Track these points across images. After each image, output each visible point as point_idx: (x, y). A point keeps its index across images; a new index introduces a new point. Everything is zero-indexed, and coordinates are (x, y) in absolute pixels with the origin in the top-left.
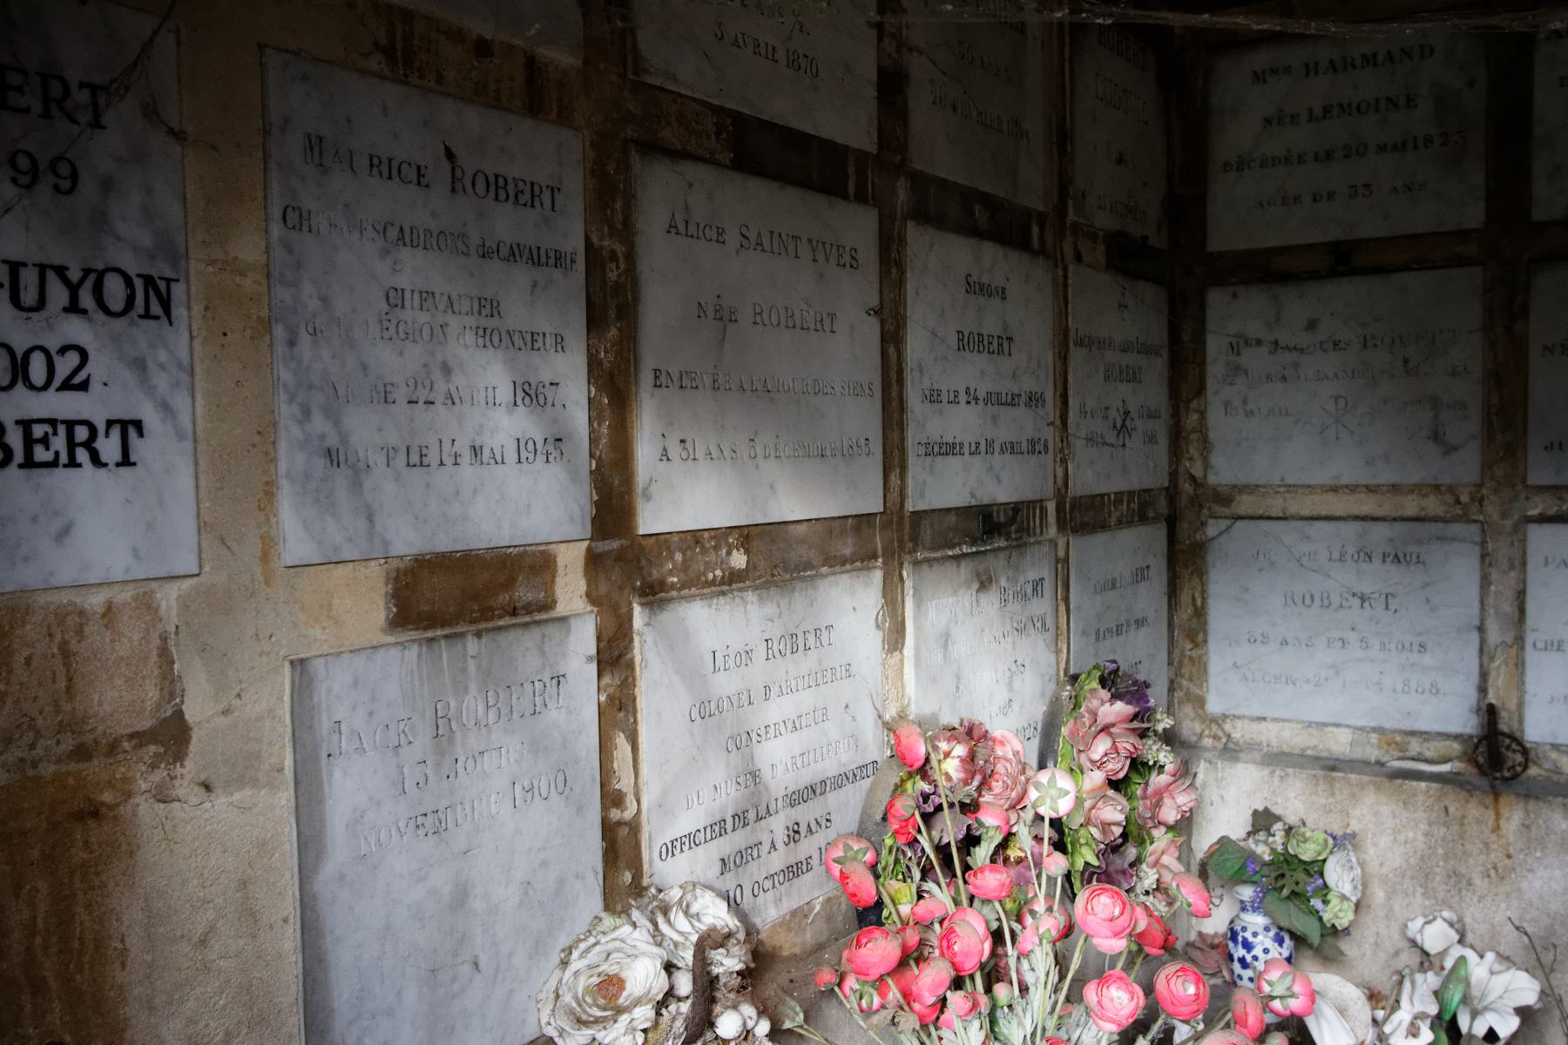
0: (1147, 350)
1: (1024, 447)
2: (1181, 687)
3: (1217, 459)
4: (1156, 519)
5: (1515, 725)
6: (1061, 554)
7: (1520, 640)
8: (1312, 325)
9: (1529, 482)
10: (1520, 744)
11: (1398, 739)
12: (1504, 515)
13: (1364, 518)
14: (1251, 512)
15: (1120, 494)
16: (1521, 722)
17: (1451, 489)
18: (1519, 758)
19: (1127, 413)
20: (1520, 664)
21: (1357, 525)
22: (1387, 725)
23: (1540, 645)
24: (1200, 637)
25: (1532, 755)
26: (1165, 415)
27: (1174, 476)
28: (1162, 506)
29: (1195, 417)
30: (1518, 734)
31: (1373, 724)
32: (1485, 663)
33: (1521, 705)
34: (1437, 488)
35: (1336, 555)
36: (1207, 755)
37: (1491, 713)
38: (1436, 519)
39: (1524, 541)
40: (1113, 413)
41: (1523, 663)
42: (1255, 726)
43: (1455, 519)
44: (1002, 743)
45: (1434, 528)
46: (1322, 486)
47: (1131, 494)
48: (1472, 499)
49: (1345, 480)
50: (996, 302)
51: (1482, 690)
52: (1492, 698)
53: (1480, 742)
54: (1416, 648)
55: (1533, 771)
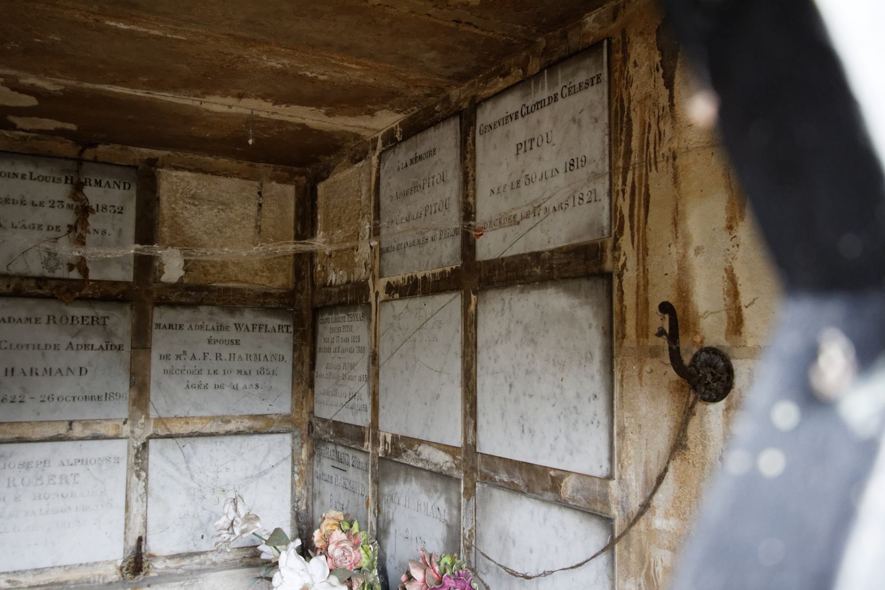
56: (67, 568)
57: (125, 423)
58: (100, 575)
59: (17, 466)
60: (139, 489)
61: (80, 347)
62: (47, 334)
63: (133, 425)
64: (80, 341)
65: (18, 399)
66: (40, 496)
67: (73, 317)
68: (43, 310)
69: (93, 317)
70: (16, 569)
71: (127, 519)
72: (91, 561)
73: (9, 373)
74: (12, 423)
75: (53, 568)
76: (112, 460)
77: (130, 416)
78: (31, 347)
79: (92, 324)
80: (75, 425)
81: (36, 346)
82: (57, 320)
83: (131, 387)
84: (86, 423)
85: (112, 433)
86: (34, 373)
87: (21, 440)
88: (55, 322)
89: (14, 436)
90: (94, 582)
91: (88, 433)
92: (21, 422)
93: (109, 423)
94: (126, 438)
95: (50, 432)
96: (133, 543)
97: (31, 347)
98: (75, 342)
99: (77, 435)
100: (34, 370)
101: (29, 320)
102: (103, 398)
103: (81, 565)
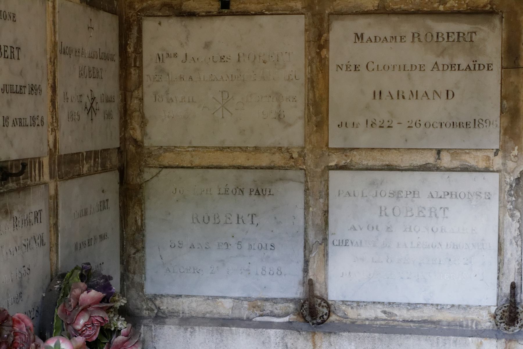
0: (105, 57)
1: (28, 122)
2: (128, 277)
3: (149, 129)
4: (111, 169)
5: (323, 291)
6: (52, 192)
7: (325, 240)
8: (207, 45)
9: (330, 146)
10: (326, 302)
11: (259, 303)
12: (317, 166)
13: (239, 168)
14: (171, 163)
15: (89, 153)
16: (326, 289)
17: (287, 149)
18: (325, 311)
19: (93, 99)
20: (326, 255)
21: (235, 172)
22: (254, 295)
23: (336, 243)
24: (140, 246)
25: (332, 308)
26: (118, 100)
27: (123, 140)
28: (115, 159)
29: (136, 101)
30: (325, 297)
31: (244, 295)
32: (307, 255)
33: (326, 278)
34: (280, 149)
35: (223, 191)
36: (145, 321)
37: (310, 284)
38: (280, 168)
39: (327, 181)
40: (85, 99)
41: (327, 254)
42: (175, 301)
43: (291, 168)
44: (19, 322)
45: (278, 173)
46: (214, 147)
47: (96, 152)
48: (300, 155)
49: (227, 144)
50: (9, 23)
51: (306, 271)
52: (311, 276)
53: (304, 303)
54: (269, 247)
55: (333, 318)
56: (439, 307)
57: (496, 154)
58: (473, 320)
59: (388, 195)
60: (513, 231)
61: (446, 67)
62: (413, 53)
63: (505, 157)
64: (446, 60)
65: (386, 124)
66: (410, 228)
67: (438, 33)
68: (407, 27)
69: (459, 33)
70: (392, 301)
71: (501, 263)
72: (464, 303)
73: (377, 96)
74: (381, 149)
75: (425, 305)
76: (483, 196)
77: (501, 146)
78: (397, 68)
79: (458, 41)
80: (443, 154)
81: (402, 67)
82: (422, 38)
83: (502, 112)
84: (455, 153)
85: (482, 165)
86: (401, 97)
87: (390, 168)
88: (420, 41)
89: (384, 163)
90: (467, 326)
91: (456, 164)
92: (389, 149)
93: (479, 154)
94: (497, 171)
95: (419, 160)
96: (507, 290)
97: (397, 68)
98: (441, 61)
99: (446, 165)
100: (401, 93)
101: (394, 38)
102: (472, 125)
103: (453, 306)
